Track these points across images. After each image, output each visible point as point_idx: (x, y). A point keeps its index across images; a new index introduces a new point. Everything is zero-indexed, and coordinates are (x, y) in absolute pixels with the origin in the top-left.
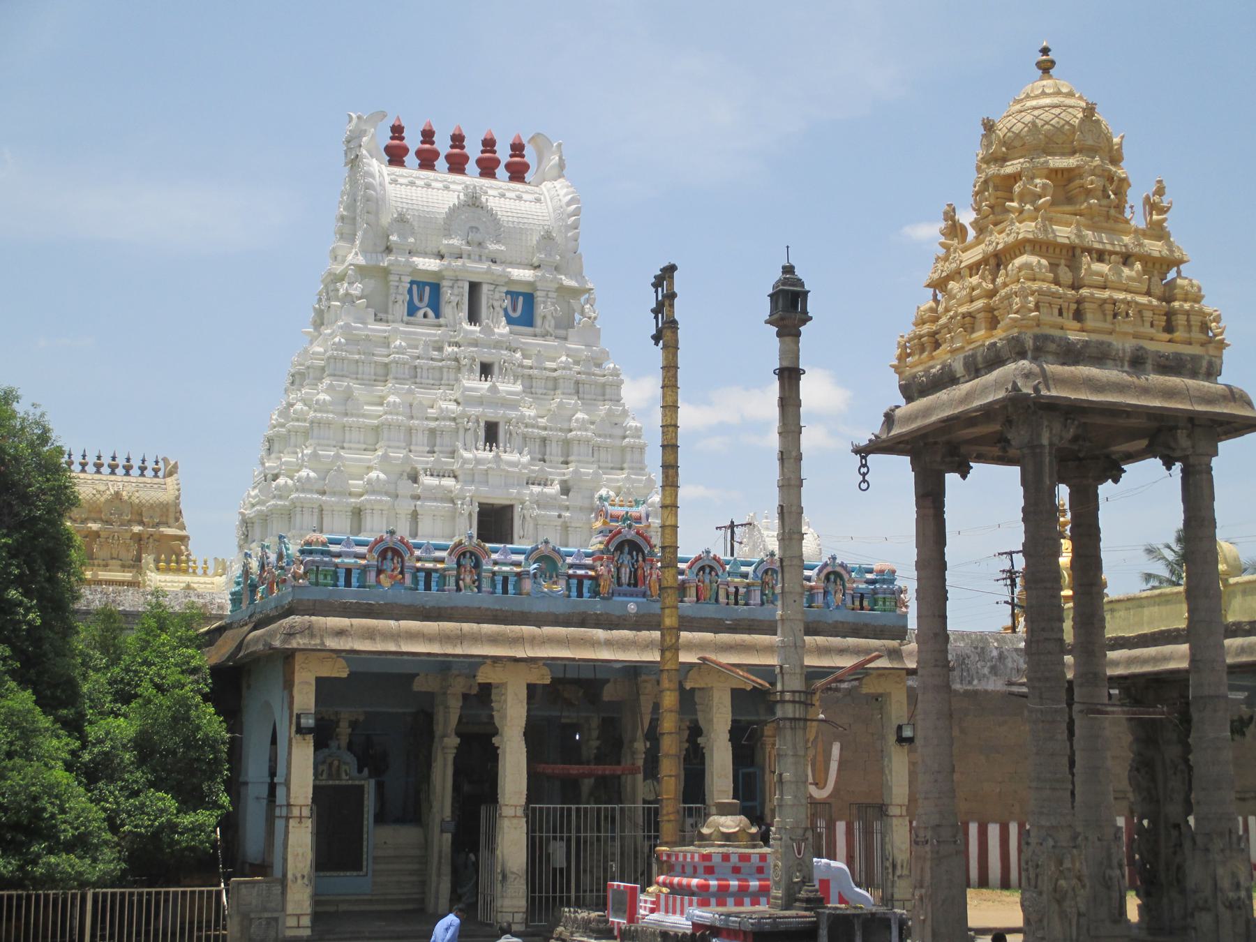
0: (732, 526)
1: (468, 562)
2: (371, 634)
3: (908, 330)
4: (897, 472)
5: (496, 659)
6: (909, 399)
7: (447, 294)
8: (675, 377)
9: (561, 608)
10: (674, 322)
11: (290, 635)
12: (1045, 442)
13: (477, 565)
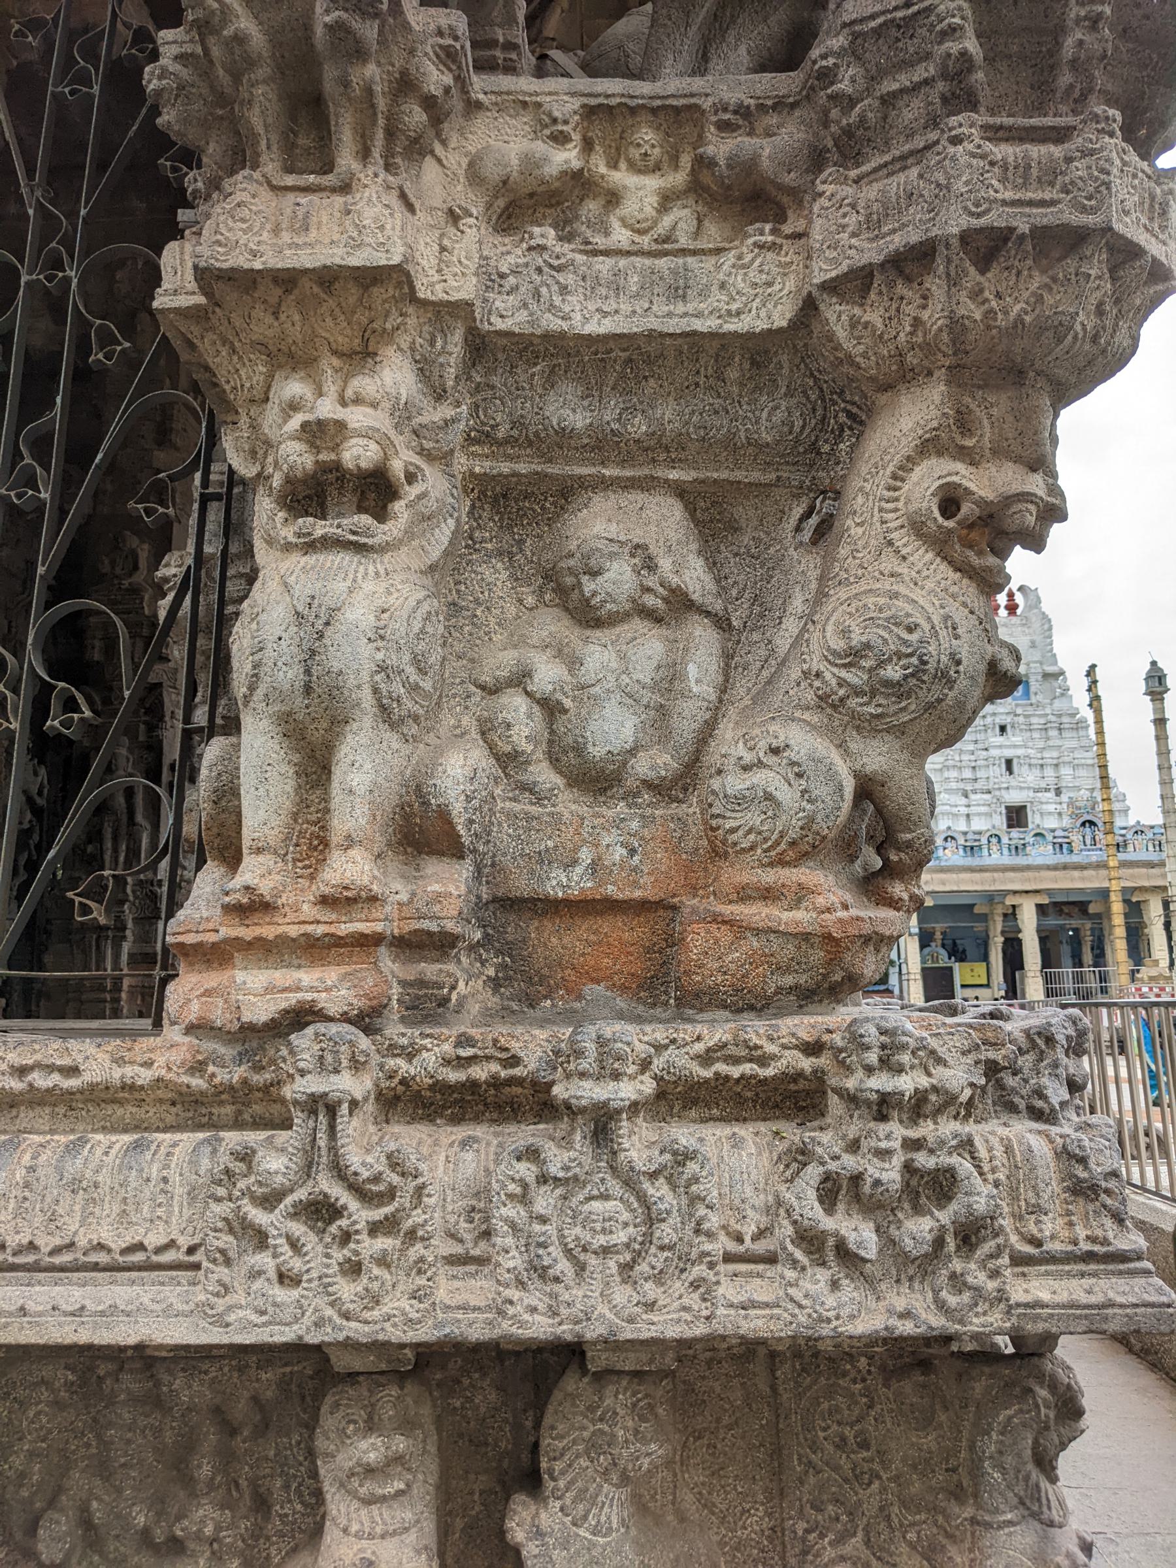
1: (994, 840)
5: (1015, 892)
13: (999, 841)
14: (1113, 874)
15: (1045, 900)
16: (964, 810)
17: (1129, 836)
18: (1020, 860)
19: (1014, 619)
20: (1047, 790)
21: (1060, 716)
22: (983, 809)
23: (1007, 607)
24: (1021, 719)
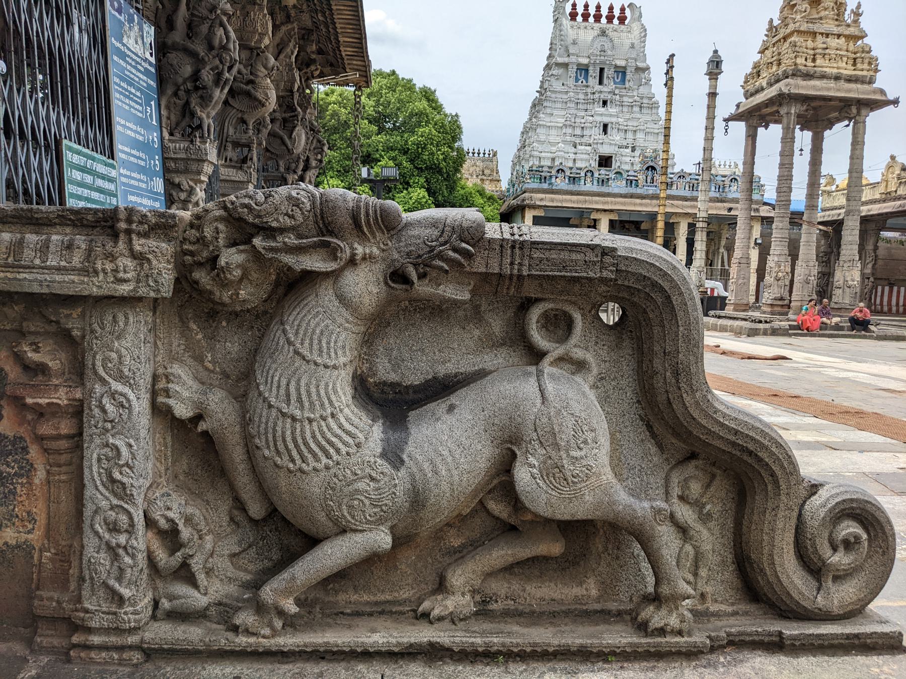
0: (699, 163)
1: (589, 174)
2: (552, 200)
3: (749, 71)
4: (739, 128)
5: (598, 210)
6: (747, 99)
7: (591, 72)
8: (671, 100)
10: (672, 78)
11: (523, 200)
12: (793, 112)
14: (662, 202)
15: (615, 217)
16: (572, 156)
17: (675, 179)
18: (604, 189)
19: (623, 27)
20: (627, 147)
21: (642, 98)
23: (618, 18)
24: (618, 97)
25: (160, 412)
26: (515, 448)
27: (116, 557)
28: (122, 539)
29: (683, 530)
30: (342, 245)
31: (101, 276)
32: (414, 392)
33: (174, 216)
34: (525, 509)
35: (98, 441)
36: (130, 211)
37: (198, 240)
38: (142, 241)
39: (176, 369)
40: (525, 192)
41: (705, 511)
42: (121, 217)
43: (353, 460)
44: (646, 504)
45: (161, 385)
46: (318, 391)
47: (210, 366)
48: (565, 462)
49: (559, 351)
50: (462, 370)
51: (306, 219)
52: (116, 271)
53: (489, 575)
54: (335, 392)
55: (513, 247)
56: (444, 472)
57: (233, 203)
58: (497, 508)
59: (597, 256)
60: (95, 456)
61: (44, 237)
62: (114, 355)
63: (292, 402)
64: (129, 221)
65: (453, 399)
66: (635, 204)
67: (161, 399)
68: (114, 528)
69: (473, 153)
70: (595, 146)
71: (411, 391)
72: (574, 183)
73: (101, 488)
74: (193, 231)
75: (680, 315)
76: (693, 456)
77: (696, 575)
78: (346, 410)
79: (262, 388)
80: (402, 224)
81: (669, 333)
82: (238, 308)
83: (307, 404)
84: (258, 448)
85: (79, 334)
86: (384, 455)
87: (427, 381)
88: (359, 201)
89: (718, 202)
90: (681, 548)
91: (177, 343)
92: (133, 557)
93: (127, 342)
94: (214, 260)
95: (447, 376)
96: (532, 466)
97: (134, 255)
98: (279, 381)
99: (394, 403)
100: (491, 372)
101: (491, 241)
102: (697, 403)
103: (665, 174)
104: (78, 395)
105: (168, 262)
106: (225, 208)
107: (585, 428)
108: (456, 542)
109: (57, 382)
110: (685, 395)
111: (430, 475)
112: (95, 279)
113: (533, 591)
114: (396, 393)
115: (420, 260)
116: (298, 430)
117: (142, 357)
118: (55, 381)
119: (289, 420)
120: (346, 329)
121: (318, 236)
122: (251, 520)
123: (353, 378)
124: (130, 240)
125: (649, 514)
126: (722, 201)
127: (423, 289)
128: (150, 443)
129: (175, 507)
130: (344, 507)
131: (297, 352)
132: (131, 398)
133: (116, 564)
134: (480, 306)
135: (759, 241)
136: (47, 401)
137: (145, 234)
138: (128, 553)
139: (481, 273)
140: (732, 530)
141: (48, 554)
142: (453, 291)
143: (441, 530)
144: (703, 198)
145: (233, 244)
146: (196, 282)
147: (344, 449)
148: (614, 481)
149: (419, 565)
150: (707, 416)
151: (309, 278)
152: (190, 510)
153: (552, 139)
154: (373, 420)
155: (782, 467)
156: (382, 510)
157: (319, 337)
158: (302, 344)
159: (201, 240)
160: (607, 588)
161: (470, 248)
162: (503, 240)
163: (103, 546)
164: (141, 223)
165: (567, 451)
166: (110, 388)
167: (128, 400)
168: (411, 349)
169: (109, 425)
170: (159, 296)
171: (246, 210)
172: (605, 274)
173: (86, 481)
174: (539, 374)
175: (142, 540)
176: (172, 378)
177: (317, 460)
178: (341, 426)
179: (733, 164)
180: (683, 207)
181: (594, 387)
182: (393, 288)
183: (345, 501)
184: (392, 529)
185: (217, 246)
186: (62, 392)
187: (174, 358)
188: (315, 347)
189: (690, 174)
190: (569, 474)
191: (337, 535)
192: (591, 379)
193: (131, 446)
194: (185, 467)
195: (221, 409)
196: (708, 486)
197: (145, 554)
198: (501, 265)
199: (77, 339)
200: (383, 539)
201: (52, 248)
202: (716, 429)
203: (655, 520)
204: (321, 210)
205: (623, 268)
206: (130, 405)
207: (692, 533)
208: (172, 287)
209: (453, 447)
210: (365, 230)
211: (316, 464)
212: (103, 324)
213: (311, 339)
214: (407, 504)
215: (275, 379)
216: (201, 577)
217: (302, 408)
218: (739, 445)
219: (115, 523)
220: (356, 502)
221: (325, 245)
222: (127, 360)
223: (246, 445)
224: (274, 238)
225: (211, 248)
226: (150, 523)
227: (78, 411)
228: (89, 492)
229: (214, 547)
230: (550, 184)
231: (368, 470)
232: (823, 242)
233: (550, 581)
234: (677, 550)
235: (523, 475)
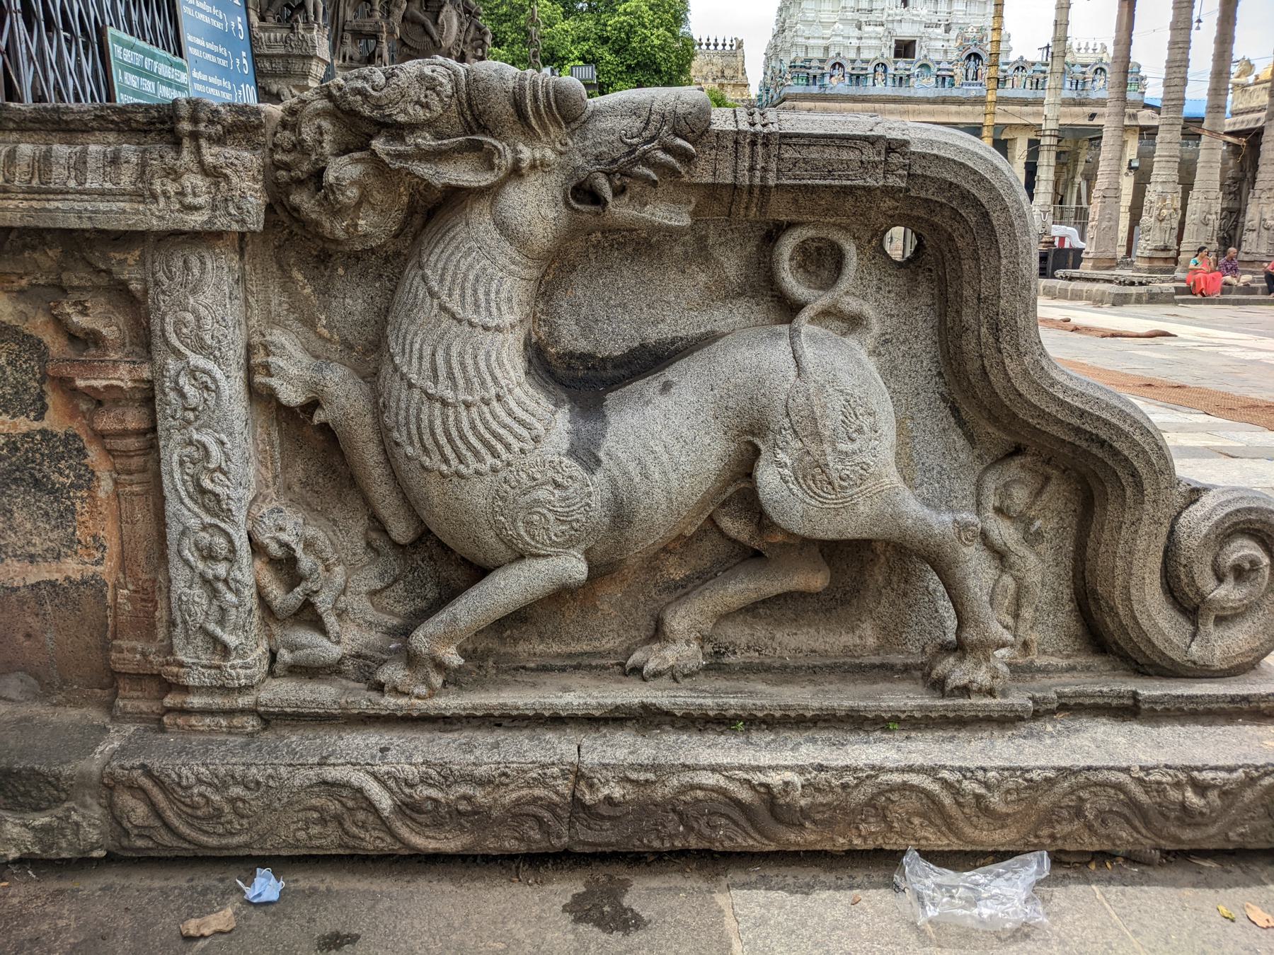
0: (1048, 47)
1: (880, 69)
9: (932, 93)
13: (885, 71)
14: (990, 108)
16: (855, 42)
17: (1010, 72)
18: (903, 92)
20: (938, 26)
22: (874, 42)
25: (260, 396)
26: (757, 441)
27: (214, 594)
28: (221, 569)
29: (1000, 556)
30: (500, 147)
31: (162, 200)
32: (615, 367)
33: (257, 112)
34: (773, 526)
35: (177, 437)
36: (195, 104)
37: (294, 146)
38: (216, 149)
39: (277, 336)
40: (784, 100)
41: (1033, 529)
42: (182, 114)
43: (530, 459)
44: (947, 518)
45: (258, 358)
46: (476, 363)
47: (325, 332)
48: (829, 458)
49: (822, 300)
50: (682, 333)
51: (446, 108)
52: (182, 194)
53: (726, 616)
54: (501, 365)
55: (753, 143)
56: (657, 476)
57: (340, 89)
58: (734, 526)
59: (879, 154)
60: (176, 458)
61: (79, 148)
62: (189, 317)
63: (441, 378)
64: (195, 120)
65: (670, 374)
66: (949, 114)
67: (259, 379)
68: (209, 555)
69: (708, 45)
70: (890, 26)
71: (609, 366)
72: (858, 84)
73: (187, 500)
74: (287, 133)
75: (1003, 240)
76: (1017, 451)
77: (1016, 616)
78: (517, 391)
79: (397, 360)
80: (587, 113)
81: (985, 269)
82: (359, 247)
83: (461, 382)
84: (397, 444)
85: (139, 287)
86: (572, 453)
87: (632, 351)
88: (523, 79)
89: (1075, 105)
90: (997, 581)
91: (278, 302)
92: (237, 592)
93: (205, 300)
94: (318, 174)
95: (659, 343)
96: (781, 465)
97: (205, 171)
98: (421, 350)
99: (586, 382)
100: (723, 335)
101: (720, 135)
102: (1026, 372)
103: (995, 64)
104: (146, 374)
105: (254, 179)
106: (330, 96)
107: (860, 410)
108: (677, 574)
109: (116, 357)
110: (1007, 361)
111: (637, 480)
112: (153, 207)
113: (786, 639)
114: (589, 369)
115: (615, 167)
116: (451, 419)
117: (229, 318)
118: (113, 356)
119: (438, 405)
120: (511, 273)
121: (465, 134)
122: (396, 545)
123: (525, 345)
124: (198, 148)
125: (951, 531)
126: (1081, 104)
127: (621, 211)
128: (250, 440)
129: (289, 527)
130: (520, 524)
131: (443, 308)
132: (218, 376)
133: (215, 602)
134: (707, 237)
135: (1135, 164)
136: (105, 383)
137: (219, 139)
138: (230, 589)
139: (706, 185)
140: (1071, 555)
141: (126, 592)
142: (666, 214)
143: (656, 556)
144: (1052, 100)
145: (344, 150)
146: (297, 209)
147: (516, 446)
148: (901, 485)
149: (627, 604)
150: (1040, 390)
151: (455, 197)
152: (310, 532)
153: (824, 17)
154: (556, 405)
155: (1149, 462)
156: (572, 528)
157: (474, 285)
158: (450, 296)
159: (298, 146)
160: (891, 634)
161: (689, 146)
162: (738, 132)
163: (196, 580)
164: (211, 122)
165: (833, 443)
166: (188, 363)
167: (214, 380)
168: (607, 304)
169: (191, 415)
170: (245, 229)
171: (359, 98)
172: (892, 181)
173: (166, 493)
174: (794, 336)
175: (248, 571)
176: (272, 348)
177: (480, 460)
178: (510, 413)
179: (1099, 47)
180: (1021, 115)
181: (874, 353)
182: (577, 211)
183: (521, 515)
184: (587, 553)
185: (321, 154)
186: (123, 370)
187: (274, 322)
188: (469, 299)
189: (1033, 64)
190: (835, 475)
191: (511, 562)
192: (870, 342)
193: (223, 443)
194: (300, 474)
195: (344, 394)
196: (1039, 493)
197: (253, 590)
198: (735, 171)
199: (138, 295)
200: (575, 567)
201: (91, 163)
202: (1052, 409)
203: (960, 538)
204: (468, 94)
205: (919, 172)
206: (217, 387)
207: (1013, 559)
208: (262, 216)
209: (670, 441)
210: (533, 122)
211: (478, 465)
212: (170, 271)
213: (463, 288)
214: (606, 520)
215: (416, 347)
216: (331, 621)
217: (455, 387)
218: (1086, 432)
219: (210, 548)
220: (536, 517)
221: (477, 147)
222: (208, 323)
223: (382, 442)
224: (402, 140)
225: (313, 157)
226: (257, 548)
227: (148, 397)
228: (172, 507)
229: (347, 582)
230: (822, 86)
231: (550, 473)
232: (1231, 163)
233: (810, 626)
234: (991, 583)
235: (769, 478)
